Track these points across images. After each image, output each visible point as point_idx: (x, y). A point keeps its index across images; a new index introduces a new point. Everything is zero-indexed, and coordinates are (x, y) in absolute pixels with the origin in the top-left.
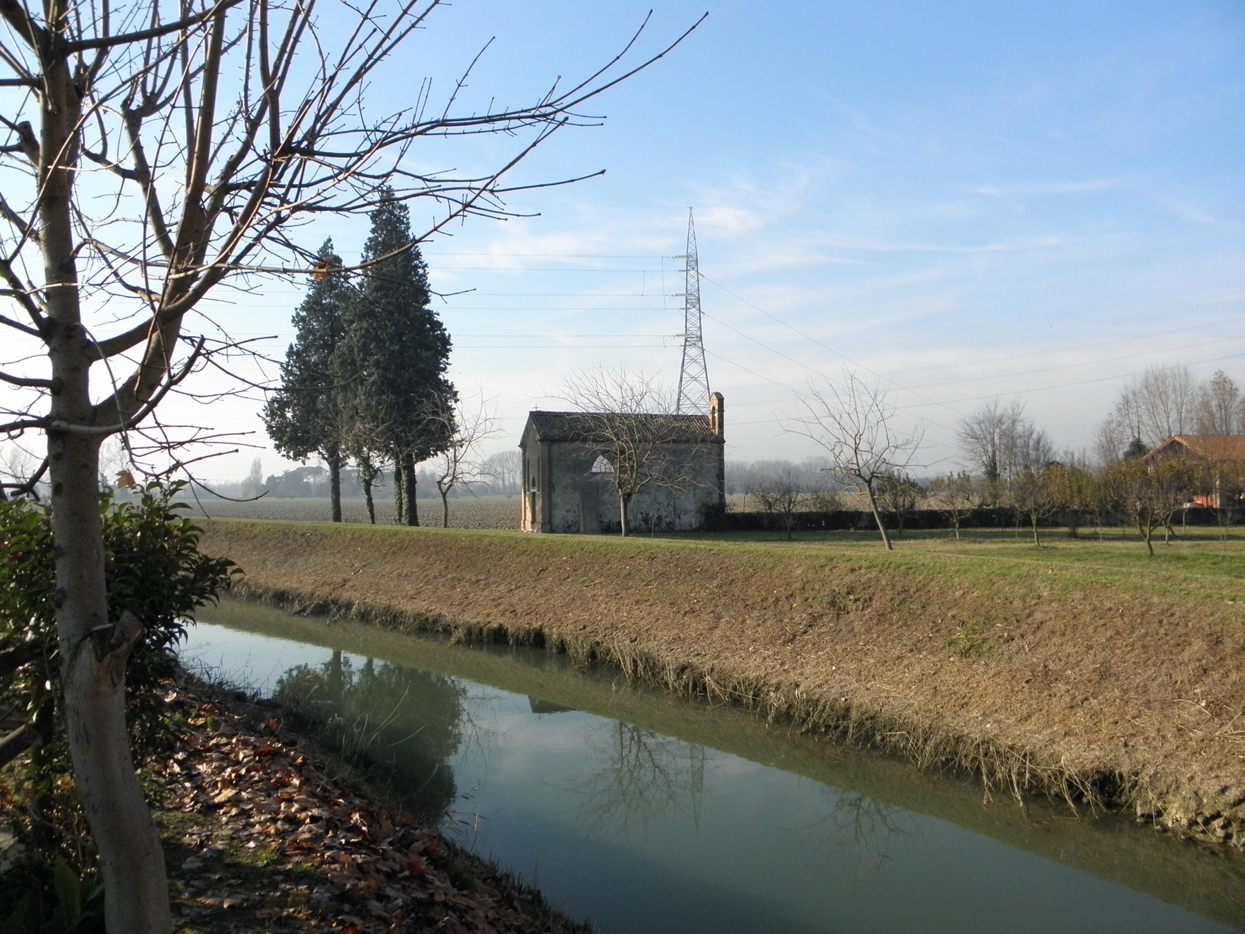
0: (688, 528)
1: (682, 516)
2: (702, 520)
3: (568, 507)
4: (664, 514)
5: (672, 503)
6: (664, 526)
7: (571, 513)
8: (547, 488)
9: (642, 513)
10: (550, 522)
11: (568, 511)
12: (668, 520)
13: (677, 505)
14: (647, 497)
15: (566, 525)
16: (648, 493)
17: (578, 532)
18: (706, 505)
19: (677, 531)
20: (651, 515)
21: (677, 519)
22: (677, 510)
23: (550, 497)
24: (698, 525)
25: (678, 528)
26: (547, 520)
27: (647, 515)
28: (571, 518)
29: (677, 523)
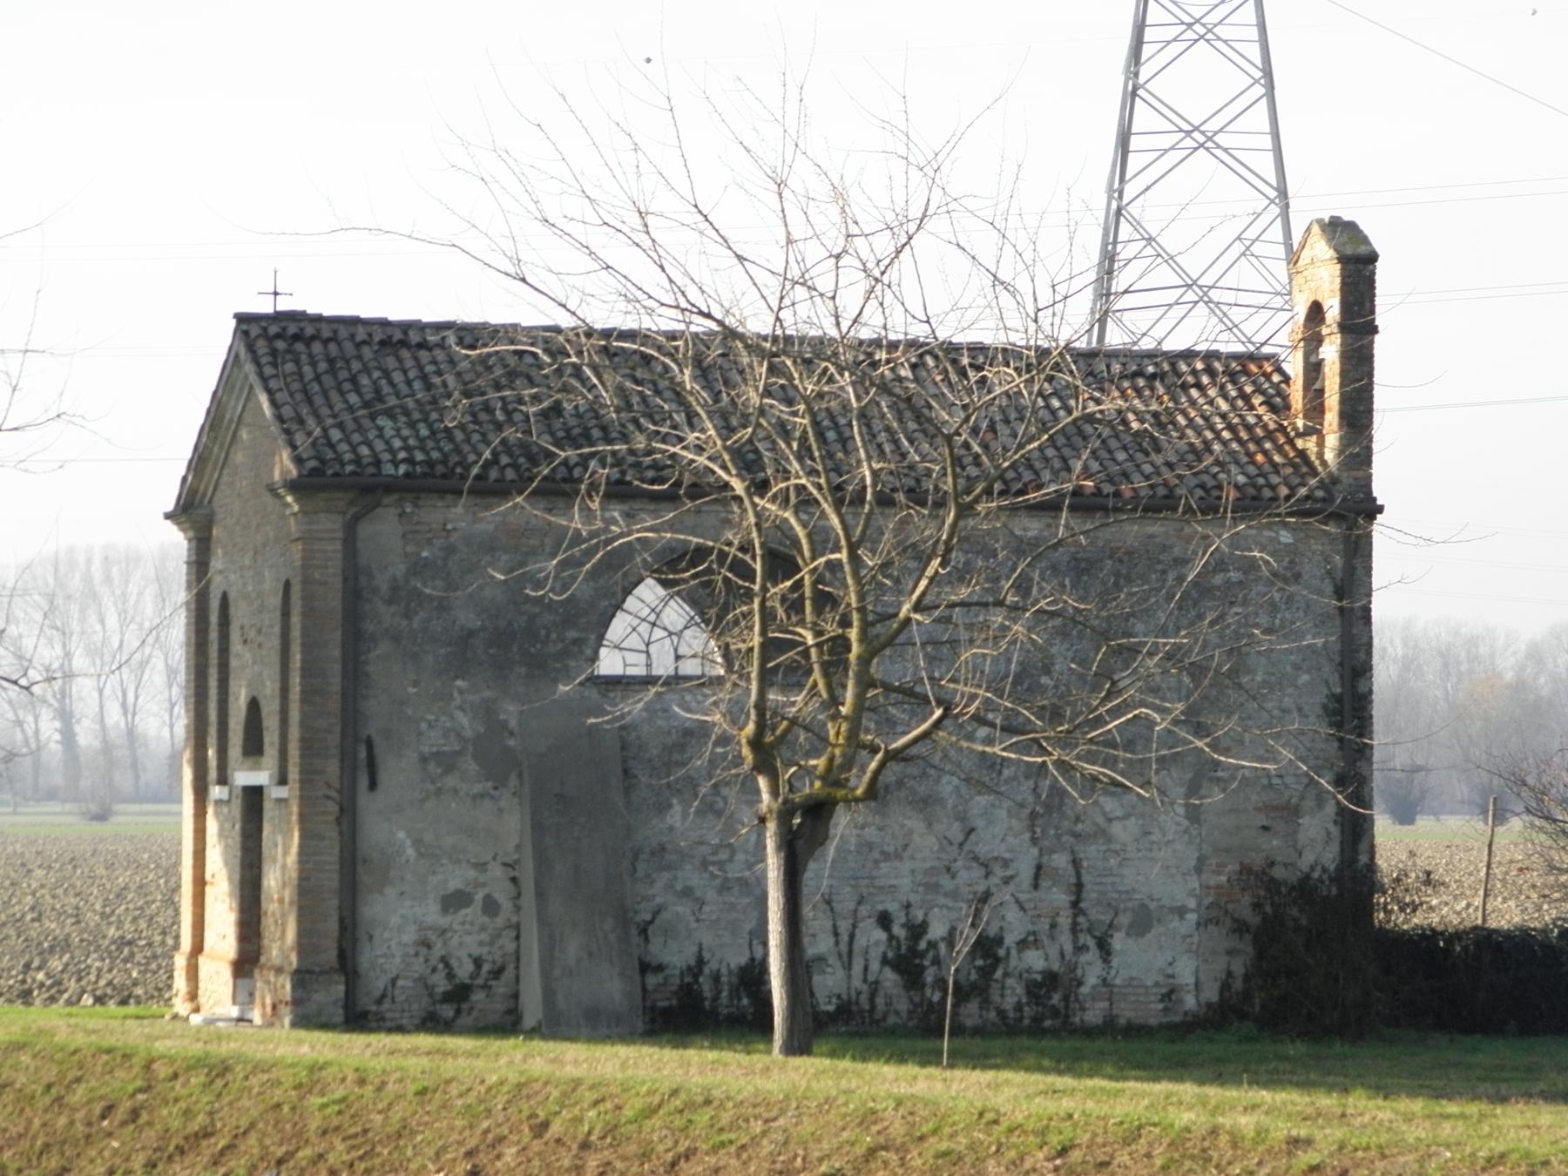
0: (1153, 1013)
1: (1118, 942)
2: (1238, 968)
3: (456, 879)
4: (1015, 925)
5: (1061, 860)
6: (1011, 994)
7: (472, 913)
8: (333, 768)
9: (884, 920)
10: (347, 965)
11: (454, 901)
12: (1035, 960)
13: (1086, 879)
14: (915, 824)
15: (441, 984)
16: (926, 804)
17: (508, 1024)
18: (1257, 878)
19: (1088, 1032)
20: (937, 931)
21: (1092, 955)
22: (1090, 894)
23: (348, 815)
24: (1211, 994)
25: (1094, 1014)
26: (330, 955)
27: (917, 930)
29: (1092, 980)
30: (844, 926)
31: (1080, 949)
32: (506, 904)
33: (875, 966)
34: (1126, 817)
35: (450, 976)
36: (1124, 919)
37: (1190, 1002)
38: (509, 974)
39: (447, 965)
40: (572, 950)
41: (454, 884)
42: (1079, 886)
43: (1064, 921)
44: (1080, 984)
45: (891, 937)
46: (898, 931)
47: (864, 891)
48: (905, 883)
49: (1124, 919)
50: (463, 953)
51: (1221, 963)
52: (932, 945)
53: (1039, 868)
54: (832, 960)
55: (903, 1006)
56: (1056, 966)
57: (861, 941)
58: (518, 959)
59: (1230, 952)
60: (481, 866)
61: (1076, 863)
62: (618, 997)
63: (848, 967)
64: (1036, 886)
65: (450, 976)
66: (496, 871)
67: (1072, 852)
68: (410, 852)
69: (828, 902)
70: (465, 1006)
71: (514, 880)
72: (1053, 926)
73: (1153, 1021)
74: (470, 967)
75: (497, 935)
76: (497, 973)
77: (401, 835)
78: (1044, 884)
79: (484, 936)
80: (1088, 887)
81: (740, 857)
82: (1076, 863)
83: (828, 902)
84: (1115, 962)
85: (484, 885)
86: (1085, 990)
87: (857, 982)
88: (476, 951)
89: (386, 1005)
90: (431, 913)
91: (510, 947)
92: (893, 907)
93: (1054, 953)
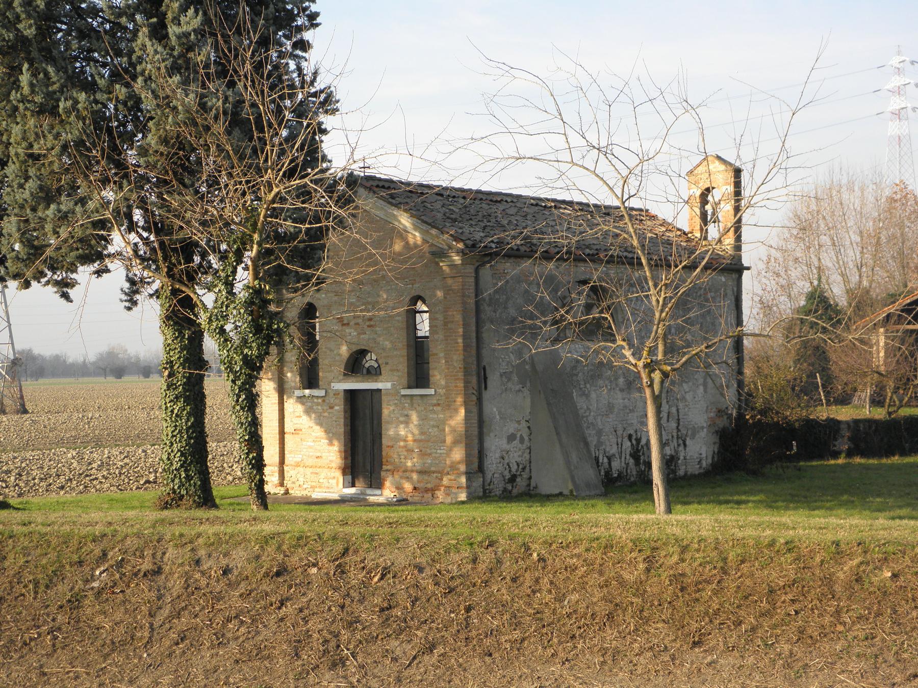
3: (511, 428)
5: (674, 410)
7: (516, 442)
8: (474, 380)
9: (630, 437)
10: (481, 469)
11: (511, 438)
13: (681, 417)
15: (508, 476)
21: (681, 448)
23: (480, 400)
25: (681, 473)
26: (476, 465)
28: (516, 455)
29: (682, 458)
30: (620, 441)
31: (679, 445)
32: (526, 438)
33: (628, 457)
34: (690, 391)
35: (510, 471)
36: (690, 433)
37: (704, 464)
38: (527, 469)
39: (509, 467)
40: (574, 457)
41: (511, 431)
42: (679, 420)
43: (675, 434)
44: (679, 459)
45: (632, 445)
46: (634, 442)
47: (625, 426)
48: (635, 422)
49: (690, 433)
50: (513, 461)
51: (711, 449)
52: (642, 446)
53: (669, 413)
54: (617, 456)
55: (634, 473)
56: (673, 453)
57: (624, 447)
58: (530, 462)
59: (714, 443)
60: (519, 422)
61: (678, 410)
62: (593, 477)
63: (621, 458)
64: (668, 421)
65: (510, 471)
66: (524, 424)
67: (677, 406)
68: (498, 417)
69: (615, 431)
70: (515, 484)
71: (529, 427)
72: (673, 437)
73: (697, 473)
74: (516, 467)
75: (523, 453)
76: (524, 469)
77: (495, 410)
78: (670, 420)
79: (520, 453)
80: (681, 420)
81: (592, 414)
82: (678, 410)
83: (615, 431)
84: (687, 449)
85: (520, 430)
86: (680, 462)
87: (623, 464)
88: (519, 460)
89: (491, 487)
90: (503, 444)
91: (527, 456)
92: (632, 432)
93: (672, 447)
